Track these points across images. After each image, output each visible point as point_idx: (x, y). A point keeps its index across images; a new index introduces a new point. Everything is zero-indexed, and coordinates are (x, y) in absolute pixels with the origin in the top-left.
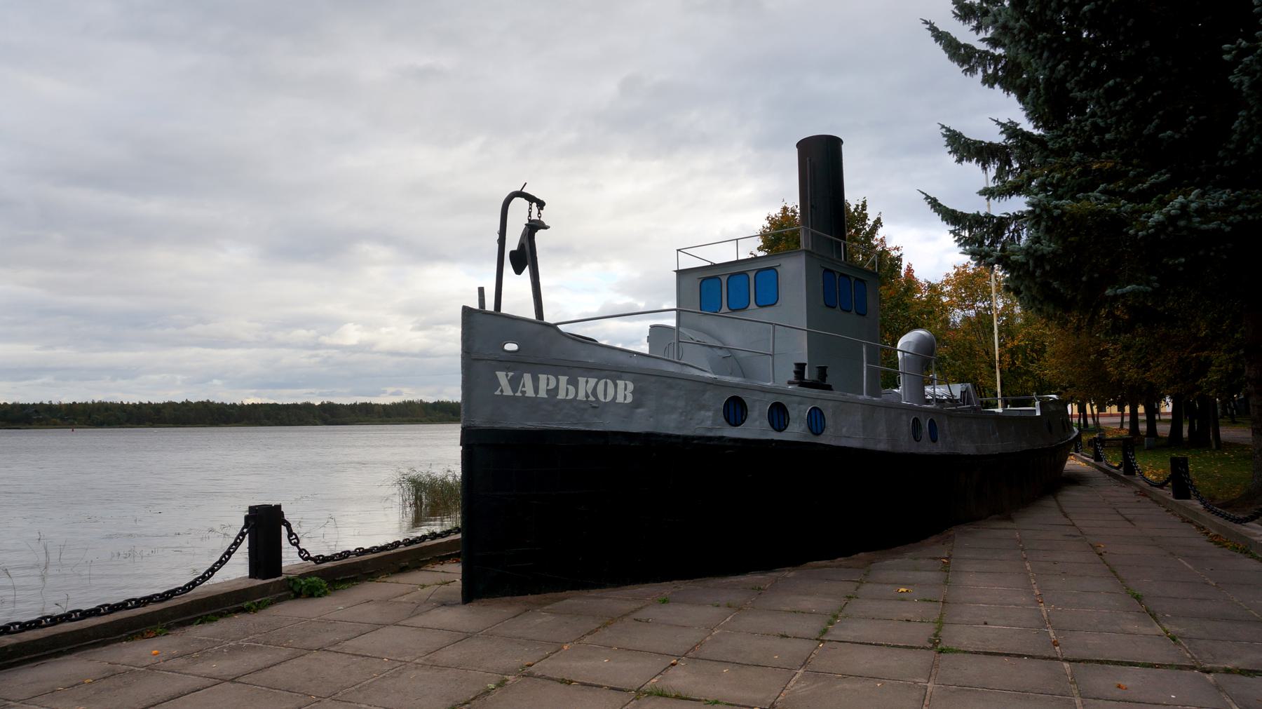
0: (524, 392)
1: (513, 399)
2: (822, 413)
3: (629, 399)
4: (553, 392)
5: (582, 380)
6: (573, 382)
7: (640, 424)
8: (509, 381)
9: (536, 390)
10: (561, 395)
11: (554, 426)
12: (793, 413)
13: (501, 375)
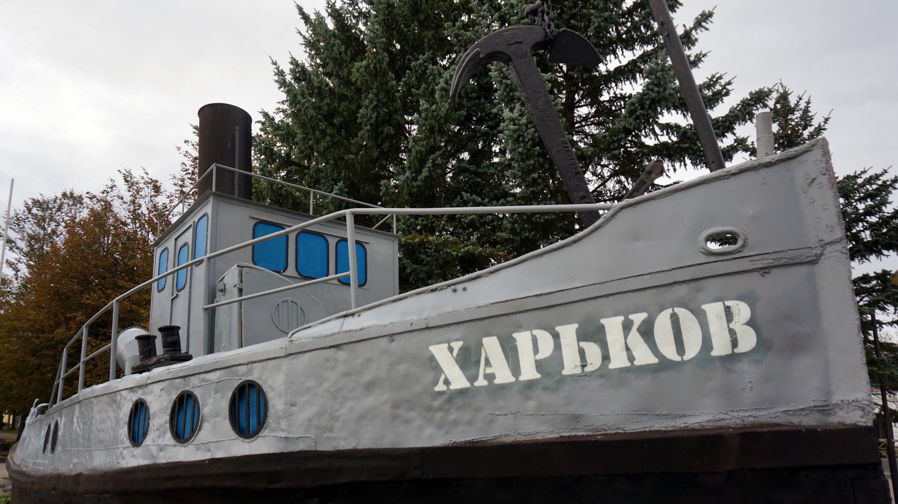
0: (490, 377)
3: (748, 341)
4: (549, 367)
9: (515, 369)
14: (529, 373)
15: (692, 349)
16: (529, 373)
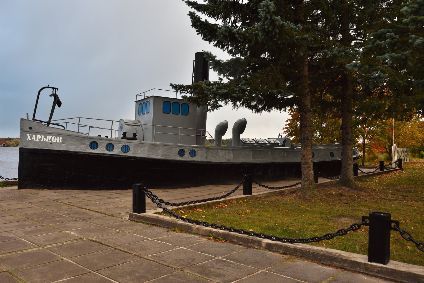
1: (31, 141)
2: (128, 146)
3: (61, 141)
5: (48, 137)
6: (45, 137)
7: (63, 148)
8: (30, 137)
9: (36, 139)
10: (42, 140)
11: (40, 148)
12: (115, 146)
13: (28, 135)
14: (37, 140)
15: (55, 141)
16: (37, 140)
